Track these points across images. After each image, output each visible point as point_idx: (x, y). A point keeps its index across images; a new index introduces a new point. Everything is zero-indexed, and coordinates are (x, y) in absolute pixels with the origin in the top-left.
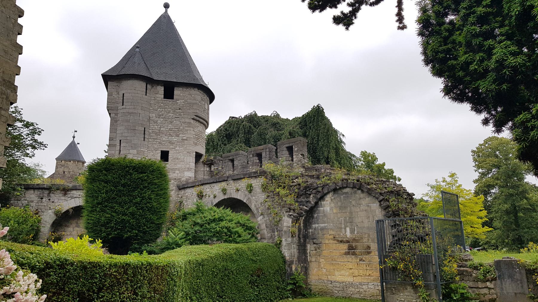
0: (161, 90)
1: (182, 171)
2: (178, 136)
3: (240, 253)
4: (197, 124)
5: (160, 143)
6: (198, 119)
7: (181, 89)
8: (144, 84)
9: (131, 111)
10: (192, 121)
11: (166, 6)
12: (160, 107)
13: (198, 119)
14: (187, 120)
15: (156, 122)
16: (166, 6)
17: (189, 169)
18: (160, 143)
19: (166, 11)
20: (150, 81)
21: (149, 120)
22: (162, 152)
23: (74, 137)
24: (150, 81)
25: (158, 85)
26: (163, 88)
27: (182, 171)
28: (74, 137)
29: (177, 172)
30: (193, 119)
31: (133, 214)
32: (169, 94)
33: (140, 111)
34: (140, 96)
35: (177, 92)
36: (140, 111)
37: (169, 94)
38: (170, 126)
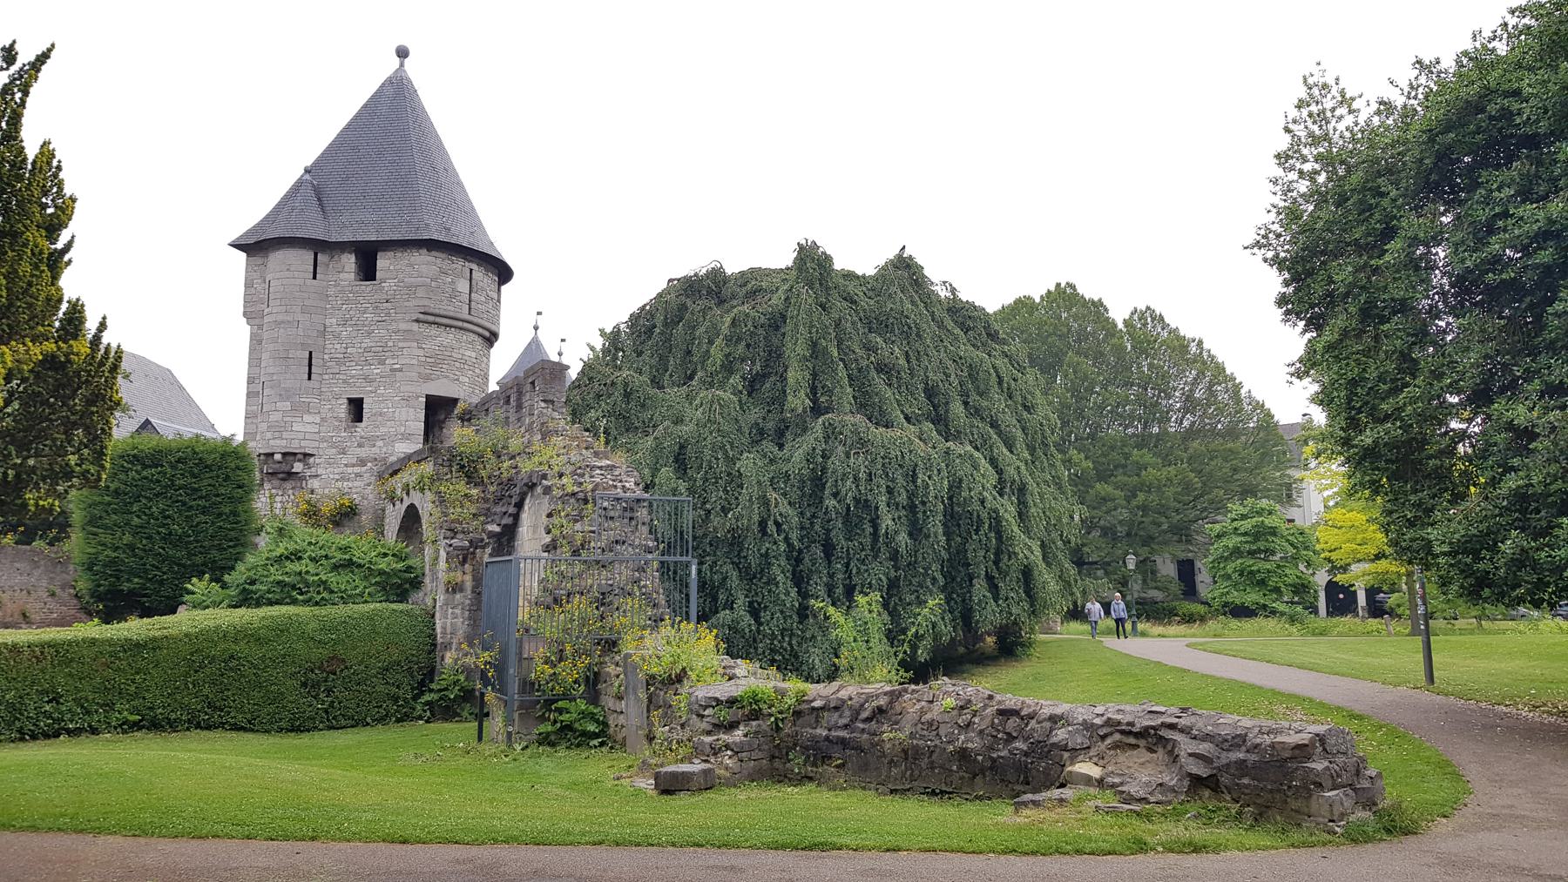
0: (349, 261)
1: (389, 440)
2: (382, 362)
3: (282, 629)
4: (434, 330)
5: (345, 381)
6: (431, 318)
7: (390, 254)
8: (308, 256)
9: (280, 318)
10: (415, 326)
11: (402, 53)
12: (347, 301)
13: (431, 318)
14: (403, 326)
15: (337, 336)
16: (402, 53)
17: (406, 437)
18: (345, 381)
19: (402, 65)
21: (323, 333)
22: (350, 400)
23: (536, 328)
24: (318, 246)
25: (343, 252)
26: (352, 258)
27: (389, 440)
28: (536, 328)
29: (380, 443)
30: (417, 321)
31: (131, 547)
32: (368, 271)
33: (300, 317)
34: (298, 282)
35: (383, 262)
36: (300, 317)
37: (368, 271)
38: (367, 343)
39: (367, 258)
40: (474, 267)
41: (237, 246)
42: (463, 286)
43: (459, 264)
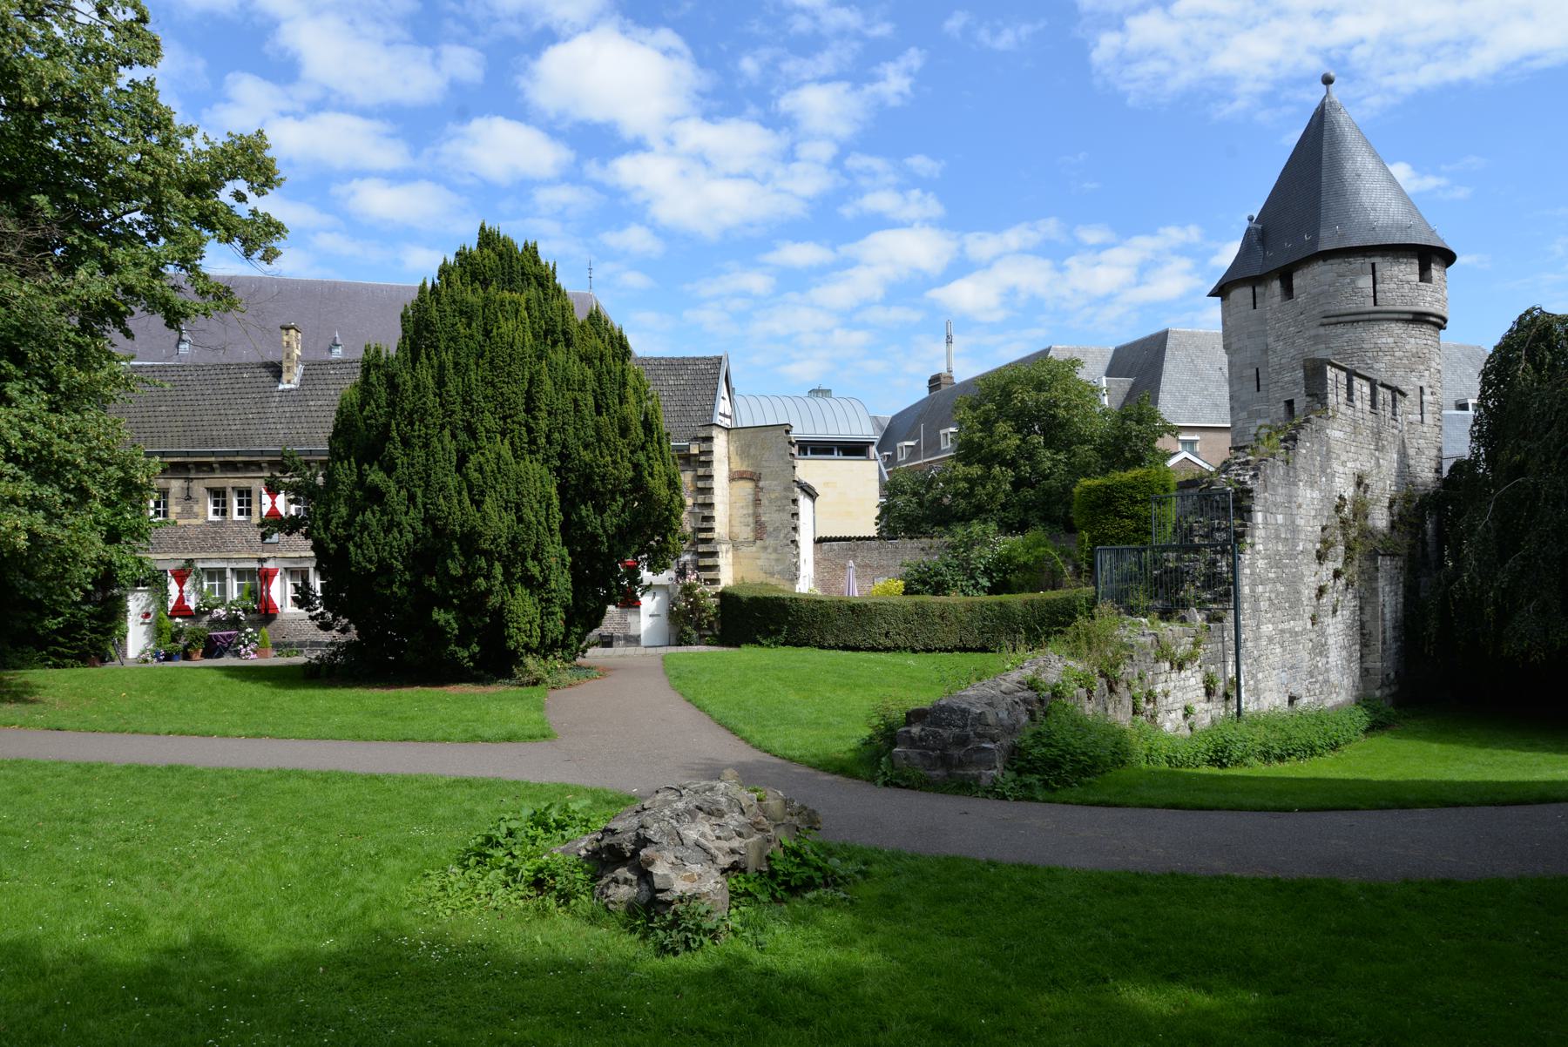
0: (1276, 286)
4: (1340, 330)
6: (1333, 320)
8: (1248, 291)
10: (1322, 331)
11: (1327, 81)
13: (1333, 320)
14: (1313, 332)
20: (1256, 281)
30: (1323, 325)
32: (1288, 291)
35: (1297, 281)
37: (1288, 291)
39: (1285, 276)
40: (1377, 260)
41: (1211, 295)
42: (1365, 282)
43: (1358, 263)
